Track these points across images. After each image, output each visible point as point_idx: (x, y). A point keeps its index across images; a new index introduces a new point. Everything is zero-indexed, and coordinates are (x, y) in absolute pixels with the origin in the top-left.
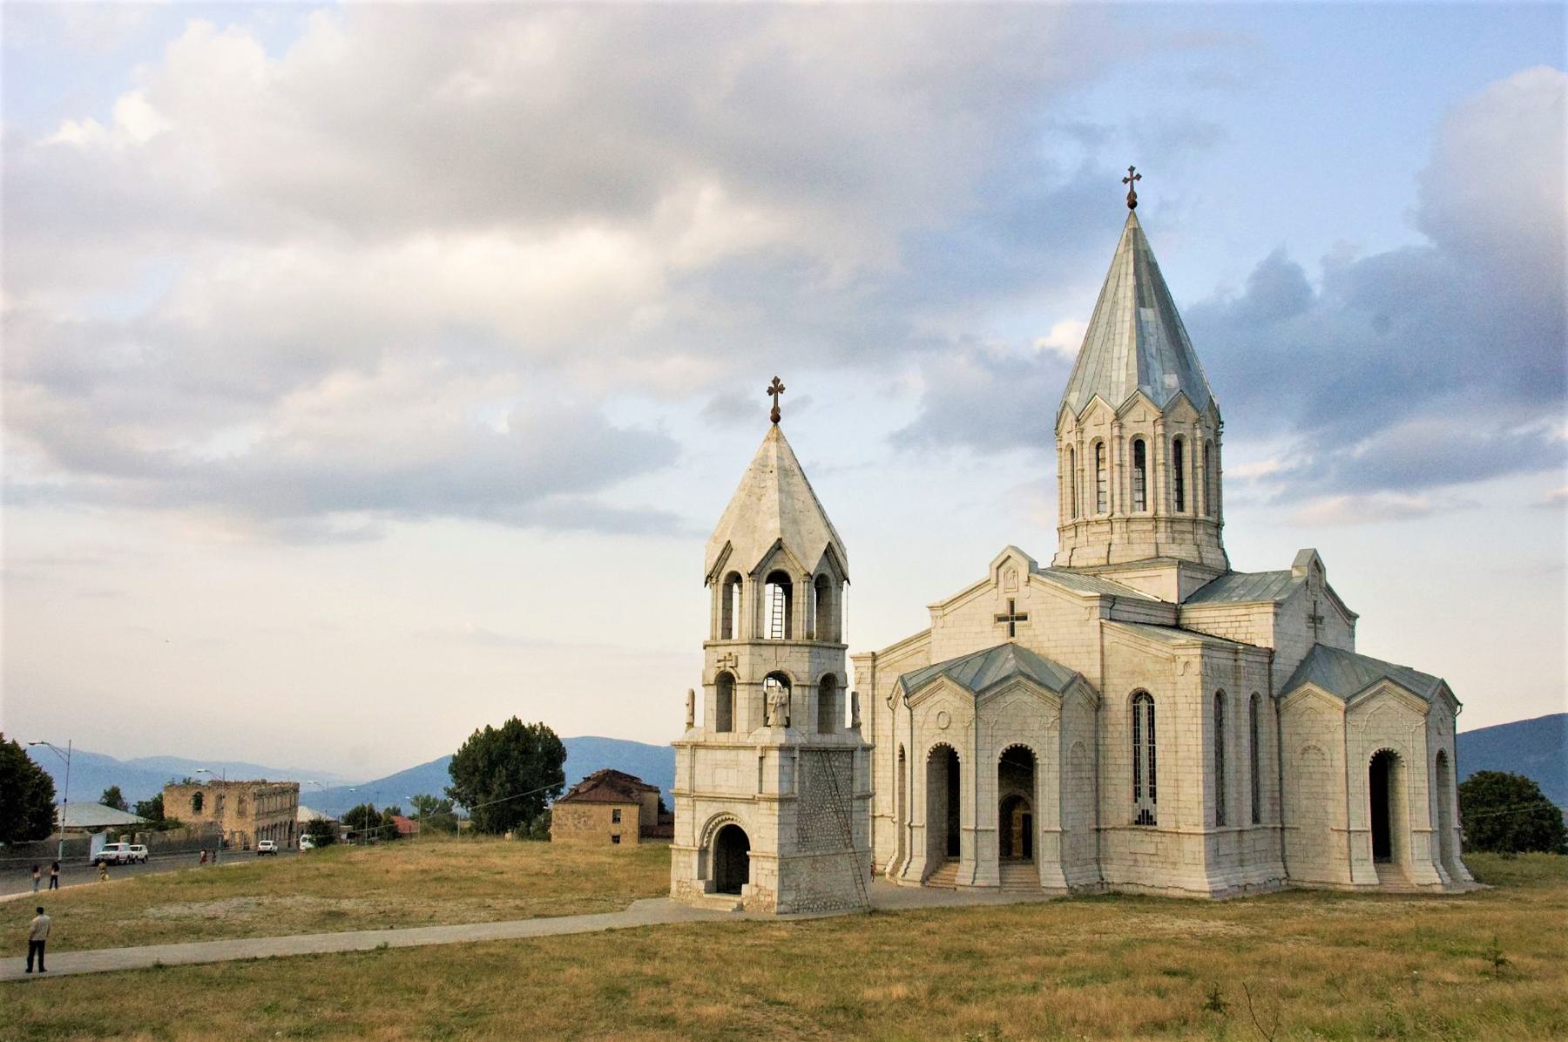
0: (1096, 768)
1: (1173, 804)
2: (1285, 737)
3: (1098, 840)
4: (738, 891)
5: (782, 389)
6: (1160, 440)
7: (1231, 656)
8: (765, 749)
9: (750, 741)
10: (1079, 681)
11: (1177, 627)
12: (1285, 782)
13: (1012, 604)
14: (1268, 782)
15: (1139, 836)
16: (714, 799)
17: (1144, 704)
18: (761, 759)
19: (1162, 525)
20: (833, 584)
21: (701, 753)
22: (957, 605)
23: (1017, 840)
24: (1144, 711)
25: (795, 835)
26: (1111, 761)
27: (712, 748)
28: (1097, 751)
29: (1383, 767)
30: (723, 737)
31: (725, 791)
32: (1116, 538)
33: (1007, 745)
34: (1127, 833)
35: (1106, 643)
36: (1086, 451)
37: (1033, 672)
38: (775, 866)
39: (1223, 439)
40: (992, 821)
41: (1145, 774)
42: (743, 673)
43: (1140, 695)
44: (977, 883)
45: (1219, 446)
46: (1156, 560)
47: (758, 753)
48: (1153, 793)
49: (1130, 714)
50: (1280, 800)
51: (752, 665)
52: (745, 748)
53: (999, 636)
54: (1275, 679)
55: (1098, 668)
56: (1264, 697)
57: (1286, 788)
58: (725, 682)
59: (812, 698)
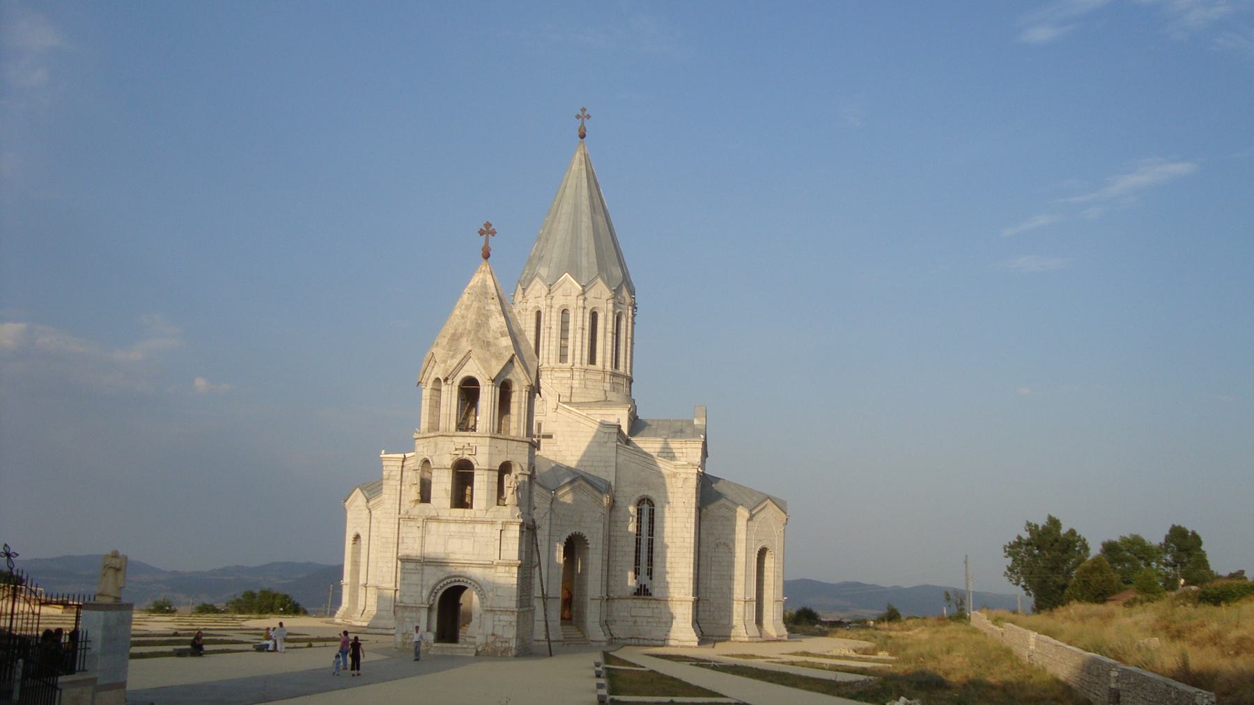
5: (493, 233)
6: (610, 314)
9: (489, 516)
15: (639, 603)
17: (646, 507)
21: (433, 526)
27: (447, 521)
33: (569, 533)
35: (620, 459)
36: (554, 314)
38: (514, 618)
47: (500, 527)
48: (650, 573)
51: (490, 454)
52: (483, 522)
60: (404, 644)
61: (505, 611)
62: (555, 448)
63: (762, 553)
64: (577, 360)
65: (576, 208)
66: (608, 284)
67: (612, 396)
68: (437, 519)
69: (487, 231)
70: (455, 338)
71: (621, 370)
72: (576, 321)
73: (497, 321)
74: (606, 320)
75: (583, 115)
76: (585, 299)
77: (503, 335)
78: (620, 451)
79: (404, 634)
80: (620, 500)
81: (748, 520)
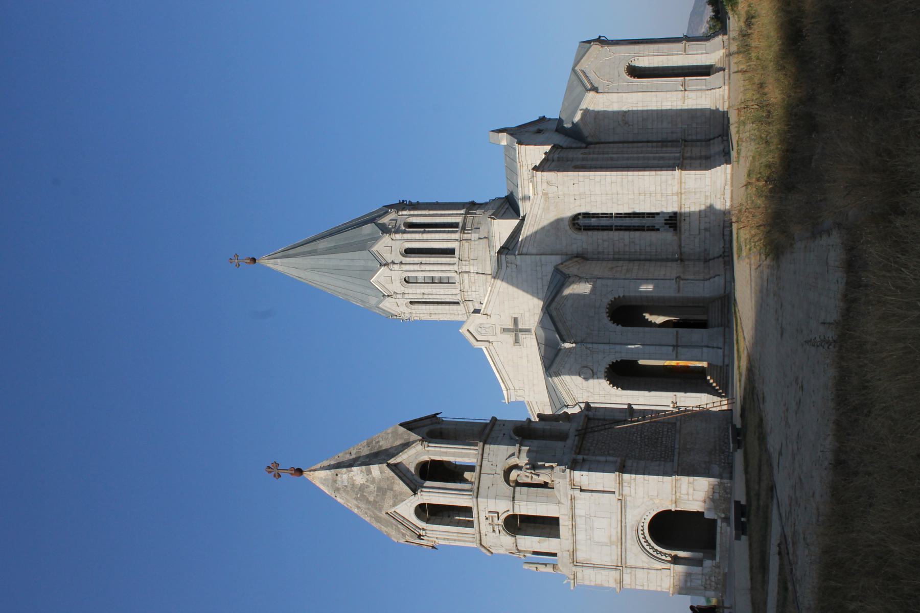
0: (630, 260)
1: (659, 196)
2: (617, 139)
3: (688, 260)
4: (714, 522)
6: (406, 236)
7: (549, 163)
8: (573, 486)
9: (567, 502)
10: (560, 267)
12: (650, 139)
13: (505, 330)
14: (650, 149)
15: (684, 226)
16: (622, 540)
17: (582, 221)
18: (582, 490)
19: (466, 236)
20: (438, 426)
21: (581, 556)
22: (507, 378)
24: (587, 222)
25: (658, 463)
26: (627, 249)
27: (574, 542)
28: (619, 260)
30: (564, 529)
31: (615, 532)
32: (473, 269)
33: (606, 320)
34: (683, 237)
35: (534, 251)
36: (411, 291)
38: (684, 480)
39: (414, 201)
41: (636, 222)
42: (504, 507)
44: (721, 345)
47: (577, 493)
48: (652, 215)
49: (590, 233)
50: (664, 143)
51: (496, 497)
52: (573, 508)
54: (574, 145)
55: (553, 257)
56: (587, 151)
57: (654, 138)
60: (716, 589)
61: (676, 490)
62: (527, 314)
63: (636, 72)
64: (451, 268)
65: (313, 269)
66: (376, 239)
67: (483, 232)
68: (574, 552)
69: (274, 469)
70: (378, 519)
71: (459, 220)
72: (414, 271)
73: (357, 475)
74: (411, 240)
76: (393, 263)
77: (369, 472)
78: (525, 251)
79: (705, 589)
80: (575, 248)
81: (597, 92)
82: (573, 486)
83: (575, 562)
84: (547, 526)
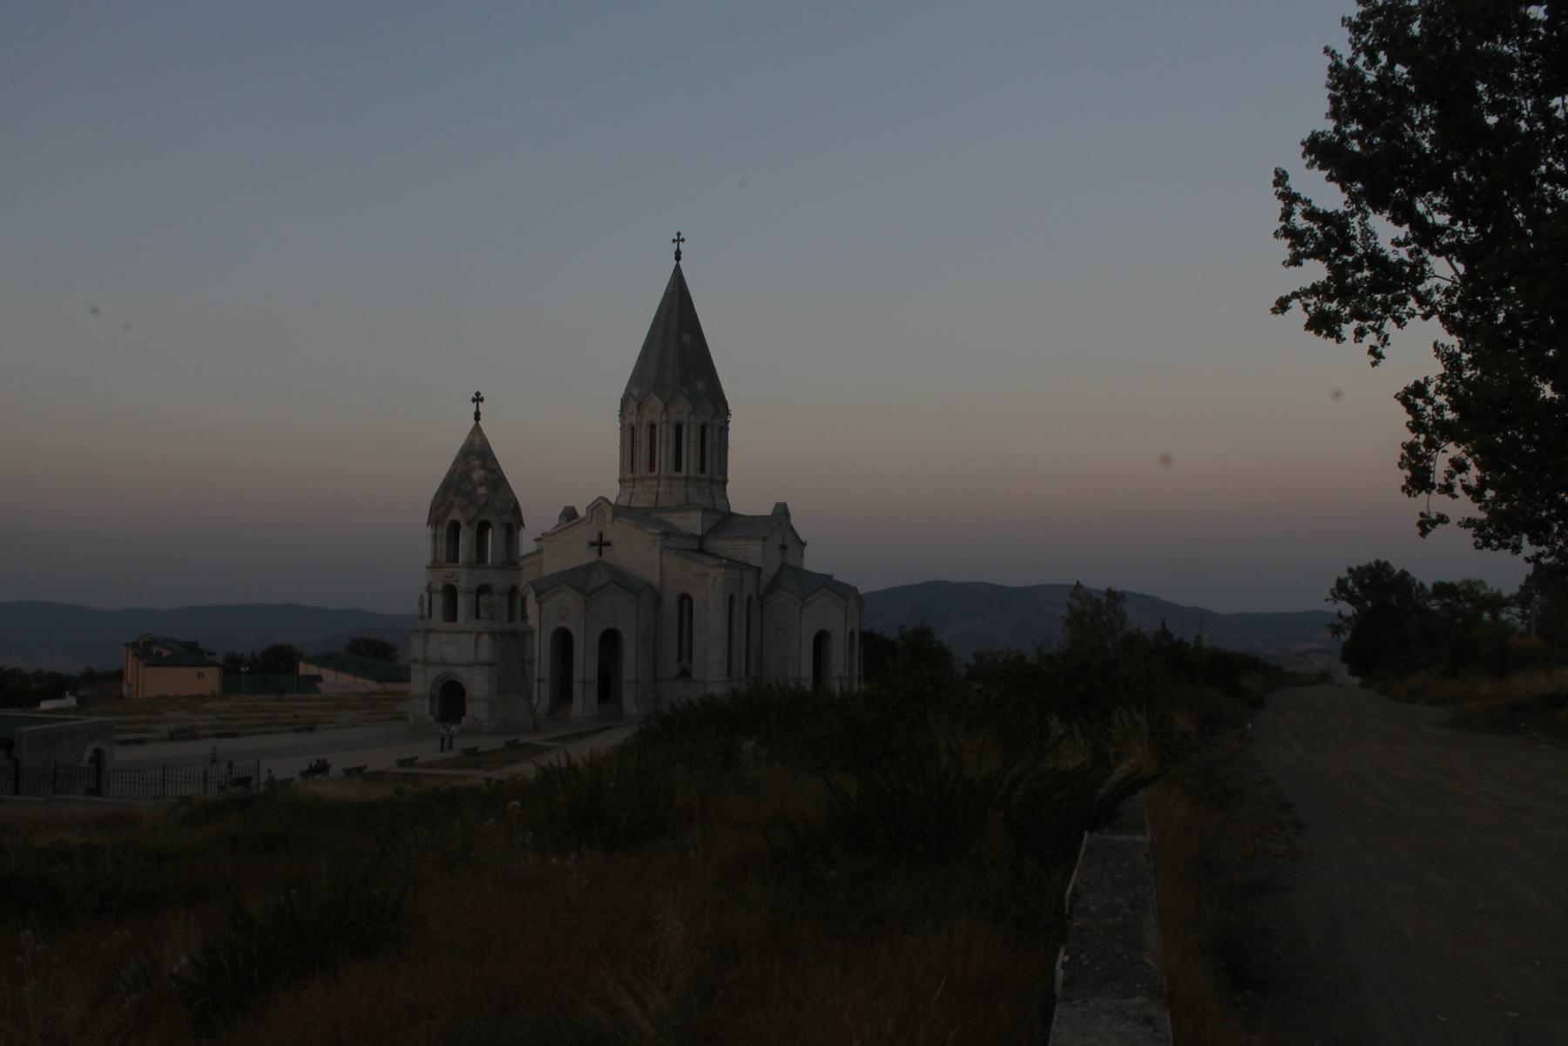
4: (459, 721)
8: (479, 633)
11: (701, 551)
13: (601, 535)
17: (686, 603)
21: (432, 636)
23: (607, 686)
29: (821, 640)
32: (661, 490)
37: (621, 580)
40: (593, 674)
41: (685, 644)
43: (685, 600)
45: (727, 429)
46: (686, 506)
48: (690, 658)
53: (590, 556)
58: (451, 592)
59: (505, 602)
75: (679, 240)
77: (481, 484)
82: (479, 633)
83: (428, 631)
84: (451, 615)
